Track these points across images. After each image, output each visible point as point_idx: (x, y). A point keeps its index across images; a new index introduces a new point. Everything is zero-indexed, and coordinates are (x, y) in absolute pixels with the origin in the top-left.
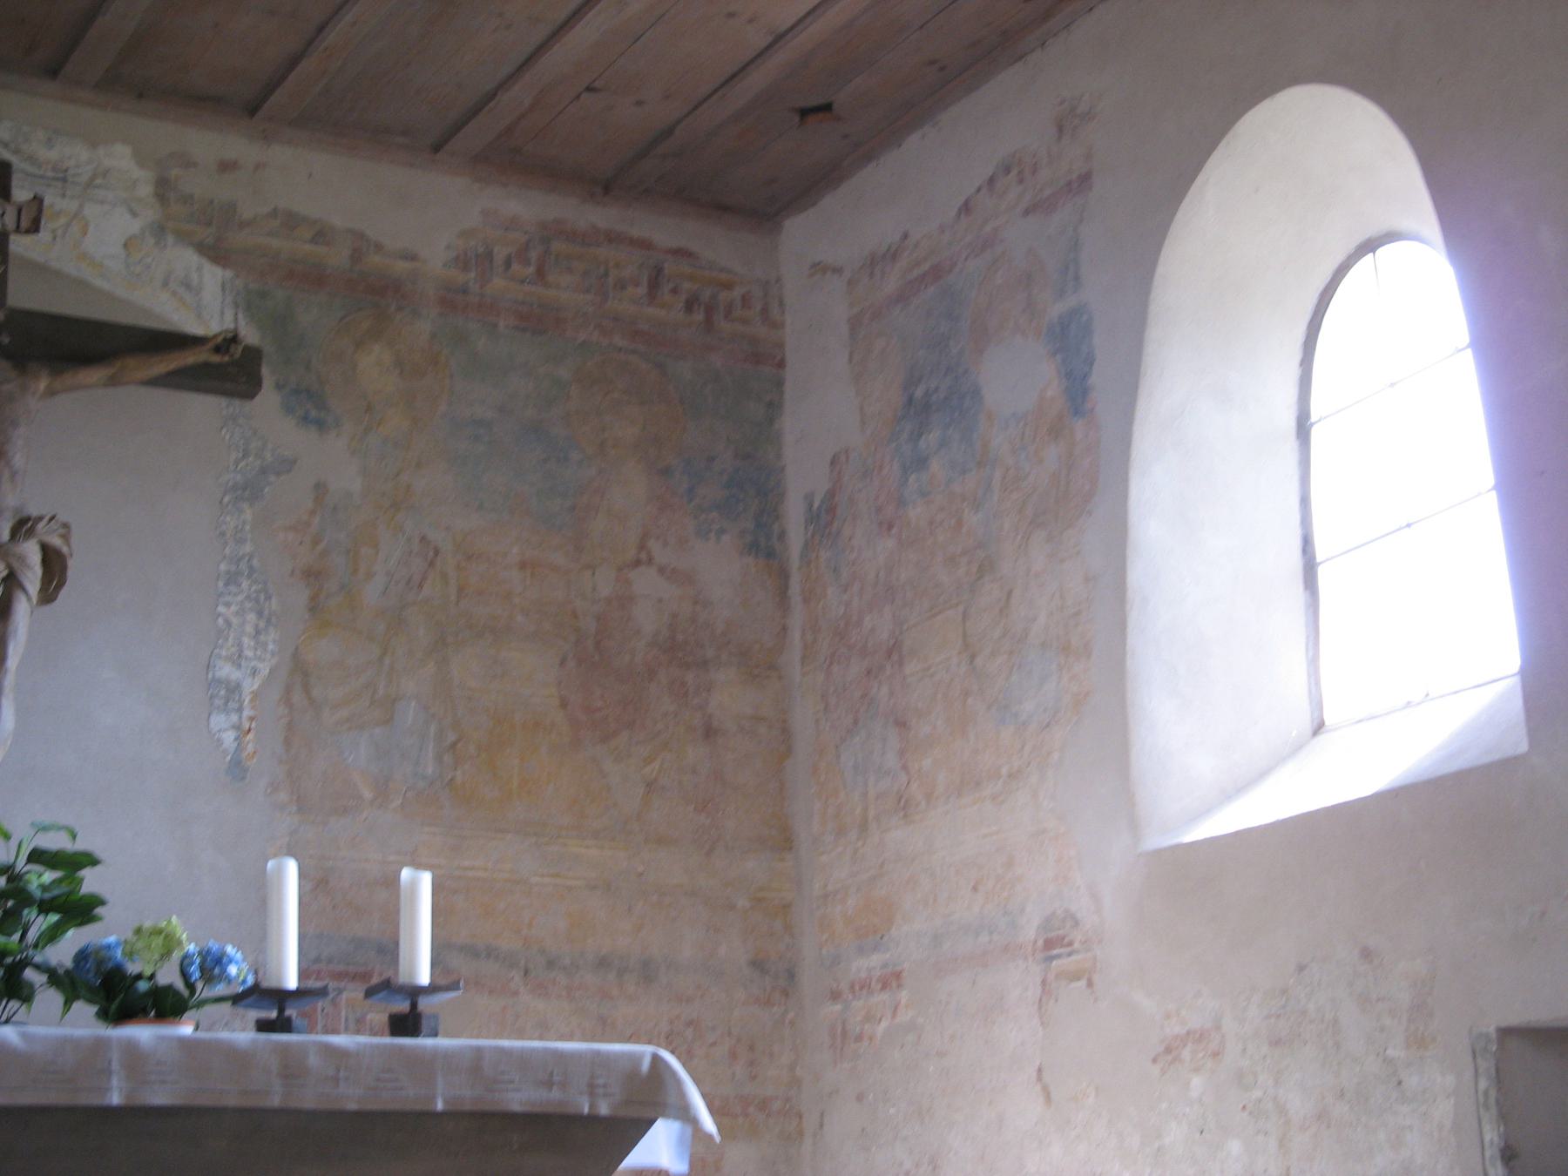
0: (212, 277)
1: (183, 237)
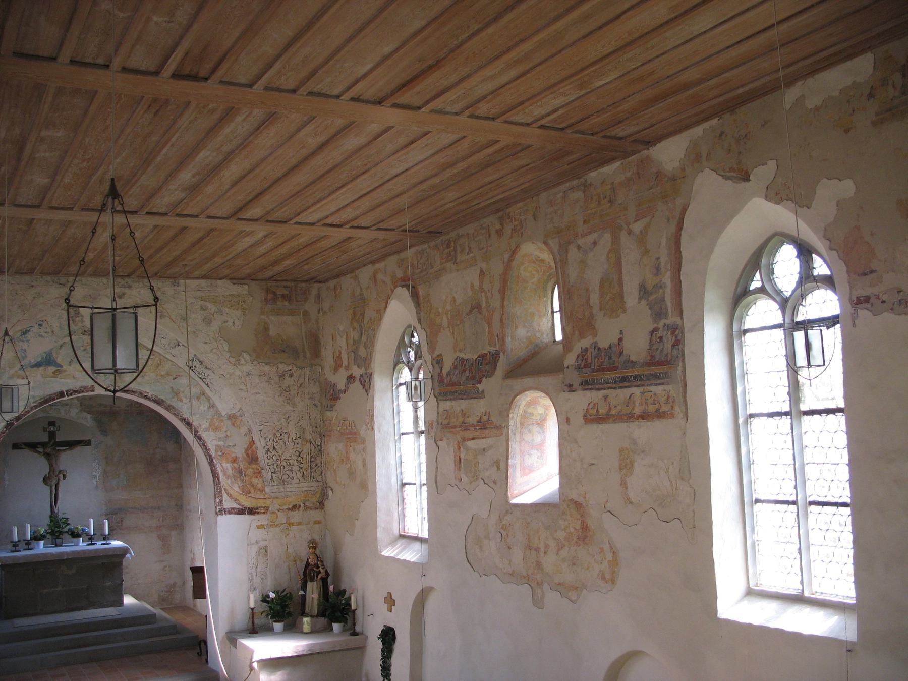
0: (89, 416)
1: (84, 411)
